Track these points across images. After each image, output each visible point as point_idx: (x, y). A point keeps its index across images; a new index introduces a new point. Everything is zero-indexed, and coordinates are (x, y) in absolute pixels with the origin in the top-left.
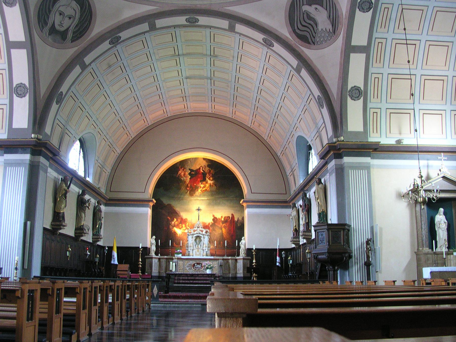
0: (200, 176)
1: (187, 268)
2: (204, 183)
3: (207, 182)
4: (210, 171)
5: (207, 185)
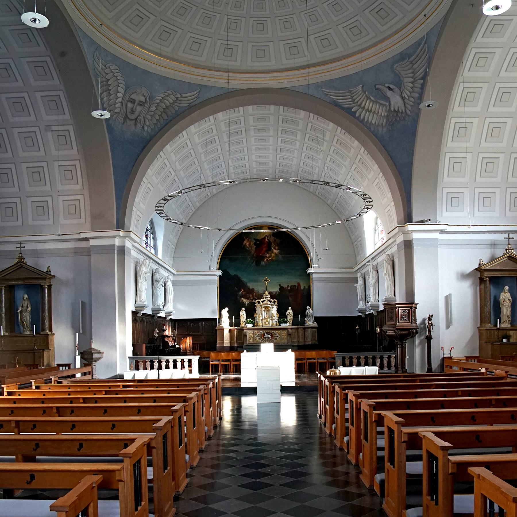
0: (265, 245)
1: (258, 338)
2: (270, 252)
3: (273, 252)
4: (275, 240)
5: (273, 255)
